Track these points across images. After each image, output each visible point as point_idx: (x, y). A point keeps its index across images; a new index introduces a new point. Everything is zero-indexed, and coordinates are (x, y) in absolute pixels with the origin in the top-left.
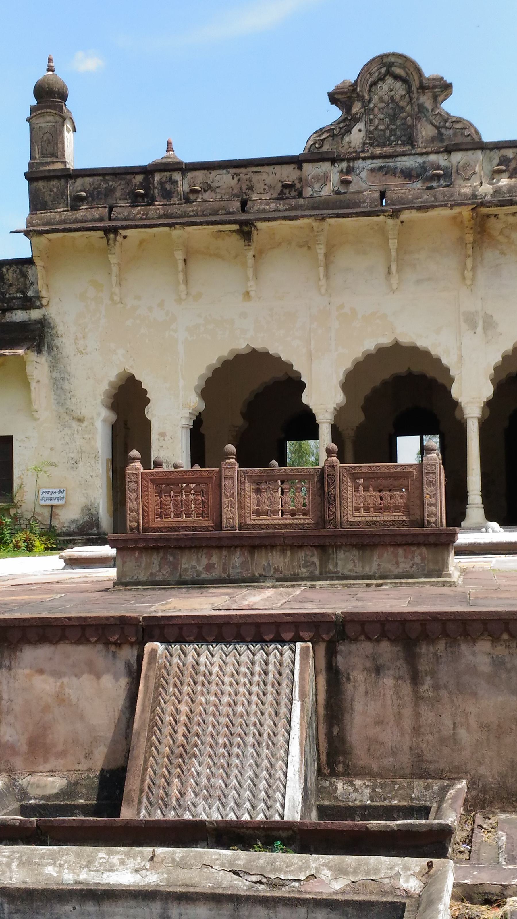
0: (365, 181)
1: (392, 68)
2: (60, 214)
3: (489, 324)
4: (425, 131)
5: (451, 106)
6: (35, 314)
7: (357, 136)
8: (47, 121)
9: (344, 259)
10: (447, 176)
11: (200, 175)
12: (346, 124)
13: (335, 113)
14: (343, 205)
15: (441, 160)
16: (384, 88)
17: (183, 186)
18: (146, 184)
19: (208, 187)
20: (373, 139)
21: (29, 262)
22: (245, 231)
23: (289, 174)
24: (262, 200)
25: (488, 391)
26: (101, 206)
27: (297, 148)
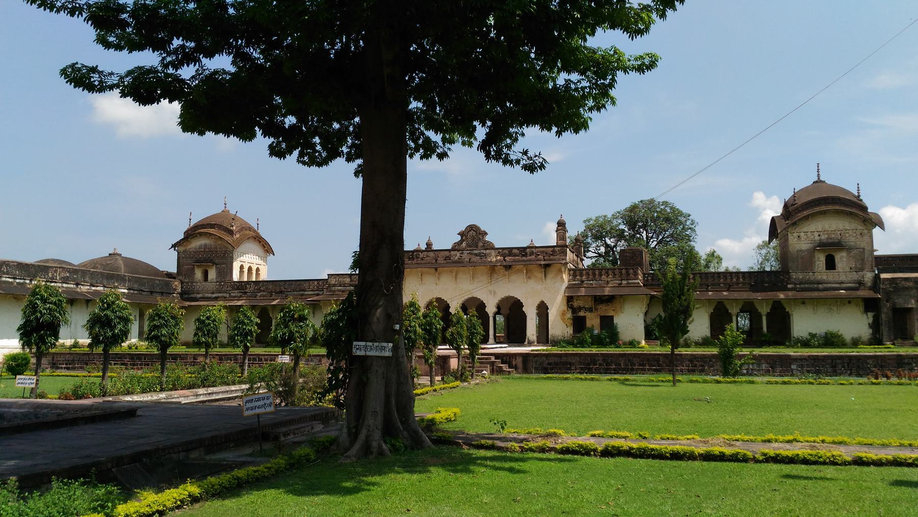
0: (466, 256)
1: (472, 228)
3: (495, 293)
4: (481, 244)
5: (487, 238)
7: (464, 245)
9: (460, 276)
10: (485, 255)
13: (459, 238)
14: (459, 263)
17: (421, 255)
18: (412, 255)
20: (468, 245)
22: (436, 269)
23: (447, 253)
24: (441, 260)
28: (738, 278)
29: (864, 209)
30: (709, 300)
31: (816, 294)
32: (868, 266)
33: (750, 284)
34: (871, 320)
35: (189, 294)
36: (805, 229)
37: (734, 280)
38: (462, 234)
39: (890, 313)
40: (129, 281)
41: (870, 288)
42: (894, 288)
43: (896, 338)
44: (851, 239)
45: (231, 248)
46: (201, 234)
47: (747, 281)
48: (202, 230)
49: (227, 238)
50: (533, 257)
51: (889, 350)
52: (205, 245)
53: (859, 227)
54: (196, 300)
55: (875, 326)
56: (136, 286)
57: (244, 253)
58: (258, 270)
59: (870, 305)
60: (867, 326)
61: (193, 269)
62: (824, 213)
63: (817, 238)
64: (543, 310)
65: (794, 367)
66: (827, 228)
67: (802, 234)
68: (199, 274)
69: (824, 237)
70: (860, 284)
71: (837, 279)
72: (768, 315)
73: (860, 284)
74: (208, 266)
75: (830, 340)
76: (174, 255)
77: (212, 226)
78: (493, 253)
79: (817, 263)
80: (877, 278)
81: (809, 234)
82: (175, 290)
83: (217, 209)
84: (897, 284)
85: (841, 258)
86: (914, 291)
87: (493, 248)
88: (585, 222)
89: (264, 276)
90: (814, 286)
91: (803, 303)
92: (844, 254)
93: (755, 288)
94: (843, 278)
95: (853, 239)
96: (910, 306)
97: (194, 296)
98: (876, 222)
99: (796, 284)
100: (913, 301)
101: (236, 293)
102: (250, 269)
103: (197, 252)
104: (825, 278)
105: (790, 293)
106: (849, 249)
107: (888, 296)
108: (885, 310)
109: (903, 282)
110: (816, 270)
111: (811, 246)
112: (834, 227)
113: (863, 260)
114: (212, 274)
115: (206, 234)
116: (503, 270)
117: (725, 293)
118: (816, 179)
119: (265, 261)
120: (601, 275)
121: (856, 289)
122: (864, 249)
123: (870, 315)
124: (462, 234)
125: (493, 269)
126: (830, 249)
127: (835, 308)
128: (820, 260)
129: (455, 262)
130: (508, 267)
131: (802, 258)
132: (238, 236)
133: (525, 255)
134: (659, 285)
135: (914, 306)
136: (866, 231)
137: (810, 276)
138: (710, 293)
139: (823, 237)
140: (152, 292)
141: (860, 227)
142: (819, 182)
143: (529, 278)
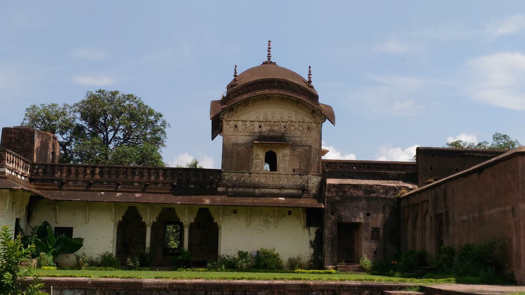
28: (158, 176)
29: (314, 97)
30: (117, 205)
31: (249, 201)
32: (314, 170)
33: (172, 184)
34: (313, 237)
36: (244, 118)
37: (153, 178)
39: (335, 228)
41: (315, 197)
42: (342, 197)
43: (339, 261)
44: (297, 134)
47: (169, 179)
51: (332, 277)
53: (307, 119)
55: (317, 245)
59: (313, 218)
60: (308, 245)
62: (267, 98)
63: (257, 130)
66: (269, 117)
67: (240, 124)
69: (265, 129)
70: (304, 190)
71: (276, 183)
72: (192, 227)
73: (304, 190)
75: (264, 262)
80: (322, 184)
81: (248, 124)
84: (344, 192)
85: (284, 155)
86: (364, 202)
90: (249, 190)
91: (235, 212)
92: (287, 151)
93: (176, 191)
94: (284, 182)
95: (298, 134)
96: (358, 220)
99: (227, 187)
100: (362, 215)
104: (263, 180)
105: (218, 199)
106: (293, 146)
107: (334, 206)
108: (329, 225)
109: (352, 191)
110: (253, 170)
111: (251, 138)
112: (277, 118)
113: (308, 160)
117: (137, 195)
121: (299, 197)
122: (310, 147)
123: (313, 230)
126: (271, 143)
127: (271, 220)
131: (238, 154)
134: (52, 181)
135: (362, 221)
136: (314, 125)
137: (246, 178)
138: (118, 194)
139: (264, 129)
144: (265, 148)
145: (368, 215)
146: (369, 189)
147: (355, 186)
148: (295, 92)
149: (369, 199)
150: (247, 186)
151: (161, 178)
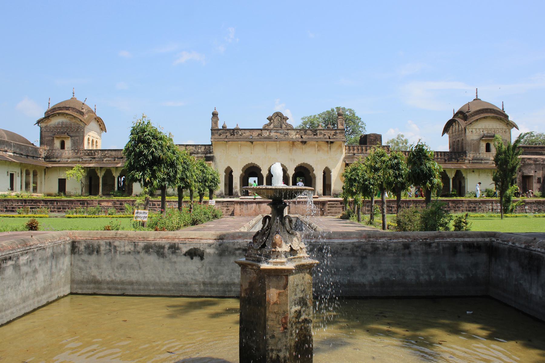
0: (273, 134)
1: (278, 115)
2: (217, 136)
3: (294, 160)
4: (284, 126)
6: (212, 155)
7: (272, 126)
8: (215, 120)
11: (243, 131)
12: (270, 124)
13: (268, 122)
15: (287, 131)
16: (277, 118)
18: (233, 132)
19: (245, 133)
20: (274, 127)
21: (211, 145)
22: (252, 143)
25: (294, 172)
26: (225, 135)
27: (261, 128)
28: (438, 156)
29: (507, 117)
35: (50, 158)
36: (475, 127)
38: (270, 119)
39: (521, 178)
40: (14, 146)
45: (82, 124)
46: (59, 114)
48: (60, 111)
49: (80, 117)
50: (322, 136)
52: (63, 123)
54: (55, 162)
56: (18, 151)
57: (91, 130)
58: (96, 142)
61: (53, 140)
63: (482, 133)
64: (327, 174)
65: (527, 207)
66: (487, 127)
67: (474, 130)
68: (57, 144)
69: (485, 132)
74: (65, 138)
76: (38, 129)
77: (67, 108)
78: (293, 133)
79: (481, 148)
81: (477, 130)
82: (40, 155)
83: (68, 97)
87: (294, 130)
88: (302, 119)
89: (99, 148)
91: (473, 171)
96: (531, 174)
97: (54, 159)
98: (512, 125)
100: (533, 172)
101: (87, 158)
102: (93, 141)
103: (56, 127)
104: (485, 156)
109: (528, 161)
111: (479, 137)
114: (68, 144)
115: (63, 114)
116: (300, 145)
118: (475, 98)
119: (100, 136)
120: (366, 150)
124: (270, 119)
125: (293, 143)
128: (483, 145)
129: (266, 138)
130: (304, 143)
132: (87, 116)
133: (316, 135)
136: (507, 130)
137: (478, 156)
140: (27, 156)
141: (505, 127)
142: (477, 99)
143: (318, 150)
144: (485, 140)
145: (536, 172)
146: (536, 160)
147: (529, 159)
148: (498, 114)
149: (535, 164)
150: (478, 160)
151: (439, 156)
